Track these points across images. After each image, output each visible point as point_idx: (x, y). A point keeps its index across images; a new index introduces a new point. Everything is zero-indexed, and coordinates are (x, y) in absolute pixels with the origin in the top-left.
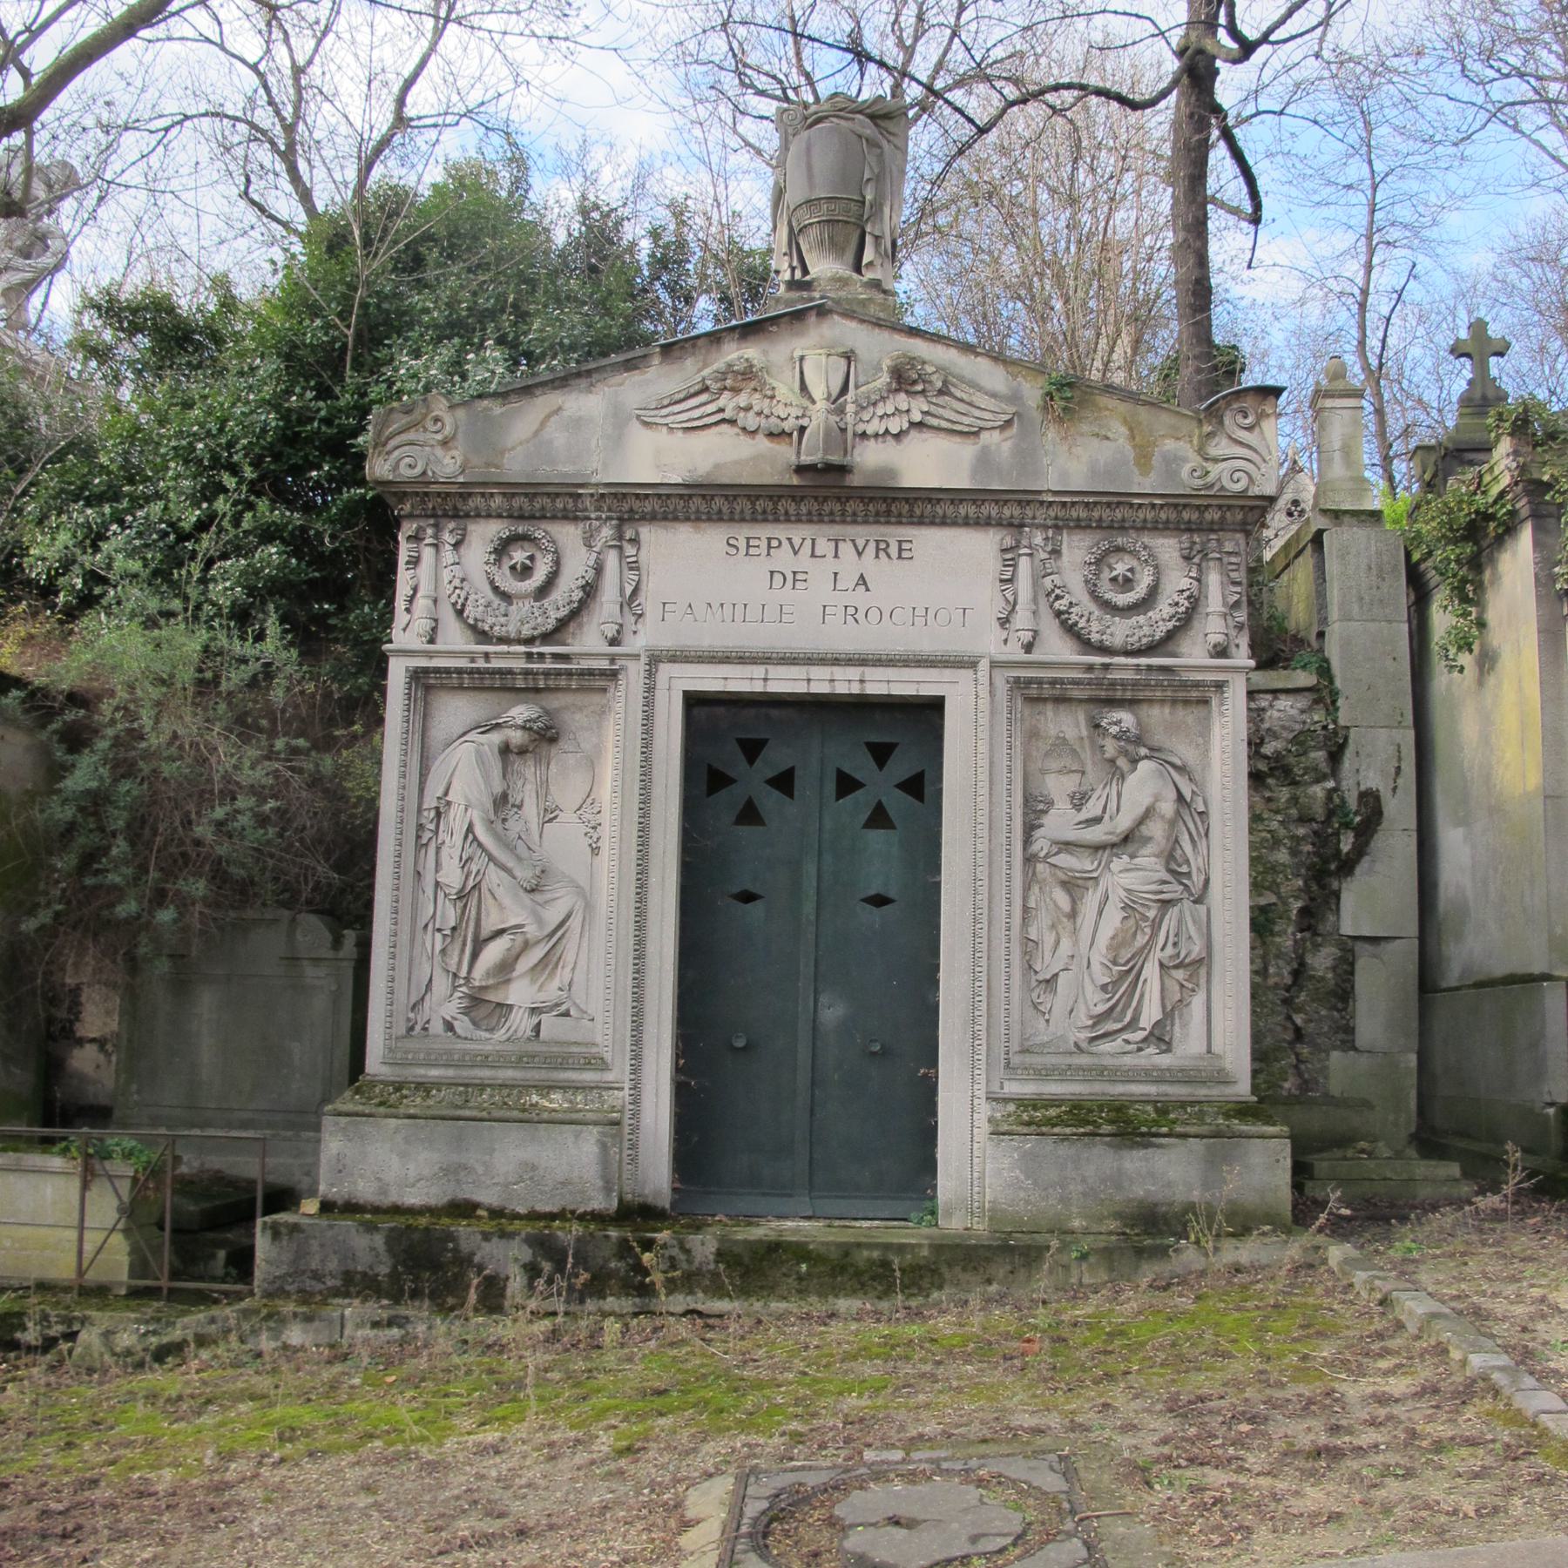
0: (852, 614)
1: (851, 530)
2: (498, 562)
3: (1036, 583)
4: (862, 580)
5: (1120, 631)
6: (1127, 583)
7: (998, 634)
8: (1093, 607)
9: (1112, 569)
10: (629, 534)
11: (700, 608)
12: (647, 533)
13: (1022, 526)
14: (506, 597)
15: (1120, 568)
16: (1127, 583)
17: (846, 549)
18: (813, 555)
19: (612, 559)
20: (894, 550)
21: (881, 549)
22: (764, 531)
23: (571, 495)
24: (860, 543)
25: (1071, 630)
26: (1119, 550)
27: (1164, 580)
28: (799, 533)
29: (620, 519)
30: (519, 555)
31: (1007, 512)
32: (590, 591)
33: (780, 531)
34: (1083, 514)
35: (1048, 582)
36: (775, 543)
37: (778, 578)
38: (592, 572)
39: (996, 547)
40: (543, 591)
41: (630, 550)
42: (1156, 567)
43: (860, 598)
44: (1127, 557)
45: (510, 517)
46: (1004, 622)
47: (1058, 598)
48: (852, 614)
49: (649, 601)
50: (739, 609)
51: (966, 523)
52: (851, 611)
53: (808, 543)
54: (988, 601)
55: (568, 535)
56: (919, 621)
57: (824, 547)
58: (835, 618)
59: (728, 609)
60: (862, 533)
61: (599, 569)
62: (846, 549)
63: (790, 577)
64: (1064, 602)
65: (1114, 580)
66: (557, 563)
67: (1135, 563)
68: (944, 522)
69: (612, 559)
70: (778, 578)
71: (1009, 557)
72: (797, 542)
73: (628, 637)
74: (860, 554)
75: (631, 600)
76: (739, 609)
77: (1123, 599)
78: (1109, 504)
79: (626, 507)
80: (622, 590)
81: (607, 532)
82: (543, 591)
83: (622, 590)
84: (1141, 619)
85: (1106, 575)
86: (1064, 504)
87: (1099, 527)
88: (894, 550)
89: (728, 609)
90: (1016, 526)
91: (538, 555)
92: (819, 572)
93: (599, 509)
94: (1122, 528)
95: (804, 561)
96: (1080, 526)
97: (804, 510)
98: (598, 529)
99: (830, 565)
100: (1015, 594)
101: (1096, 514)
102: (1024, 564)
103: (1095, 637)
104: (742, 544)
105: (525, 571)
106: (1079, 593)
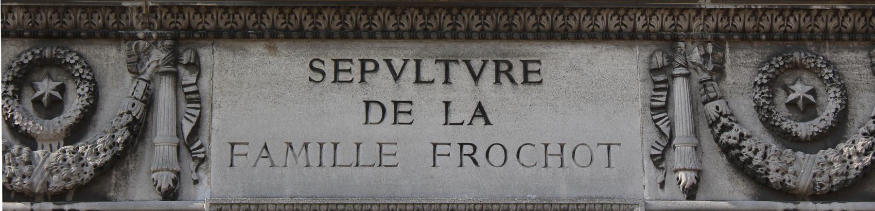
0: (469, 152)
1: (464, 48)
2: (17, 95)
3: (695, 112)
4: (480, 111)
5: (805, 169)
6: (807, 109)
7: (651, 173)
8: (768, 139)
9: (788, 91)
10: (186, 58)
11: (278, 151)
12: (207, 55)
13: (675, 39)
14: (28, 140)
15: (800, 90)
16: (807, 109)
17: (459, 72)
18: (418, 81)
19: (165, 91)
20: (518, 73)
21: (503, 71)
22: (355, 51)
23: (113, 9)
24: (476, 64)
25: (742, 167)
26: (796, 67)
27: (853, 103)
28: (399, 53)
29: (176, 39)
30: (46, 87)
31: (656, 24)
32: (139, 129)
33: (376, 51)
34: (750, 25)
35: (711, 107)
36: (370, 66)
37: (376, 110)
38: (139, 107)
39: (643, 67)
40: (76, 132)
41: (188, 78)
42: (843, 87)
43: (478, 133)
44: (805, 76)
45: (34, 35)
46: (658, 161)
47: (725, 128)
48: (469, 152)
49: (216, 146)
50: (328, 149)
51: (606, 37)
52: (468, 149)
53: (411, 65)
54: (633, 130)
55: (109, 59)
56: (553, 161)
57: (431, 70)
58: (448, 164)
59: (313, 149)
60: (477, 51)
61: (149, 101)
62: (459, 72)
63: (390, 108)
64: (733, 133)
65: (792, 105)
66: (95, 94)
67: (817, 83)
68: (579, 36)
69: (165, 91)
70: (376, 110)
71: (660, 79)
72: (397, 64)
73: (187, 188)
74: (476, 78)
75: (190, 143)
76: (328, 149)
77: (804, 129)
78: (781, 12)
79: (184, 23)
80: (179, 127)
81: (158, 55)
82: (76, 132)
83: (179, 127)
84: (831, 154)
85: (781, 98)
86: (726, 12)
87: (769, 39)
88: (518, 73)
89: (313, 149)
90: (669, 40)
91: (71, 85)
92: (427, 103)
93: (150, 26)
94: (799, 37)
95: (407, 88)
96: (745, 37)
97: (406, 26)
98: (147, 52)
99: (440, 92)
100: (671, 126)
101: (765, 24)
102: (680, 87)
103: (774, 177)
104: (329, 69)
105: (51, 107)
106: (749, 121)
